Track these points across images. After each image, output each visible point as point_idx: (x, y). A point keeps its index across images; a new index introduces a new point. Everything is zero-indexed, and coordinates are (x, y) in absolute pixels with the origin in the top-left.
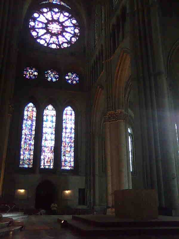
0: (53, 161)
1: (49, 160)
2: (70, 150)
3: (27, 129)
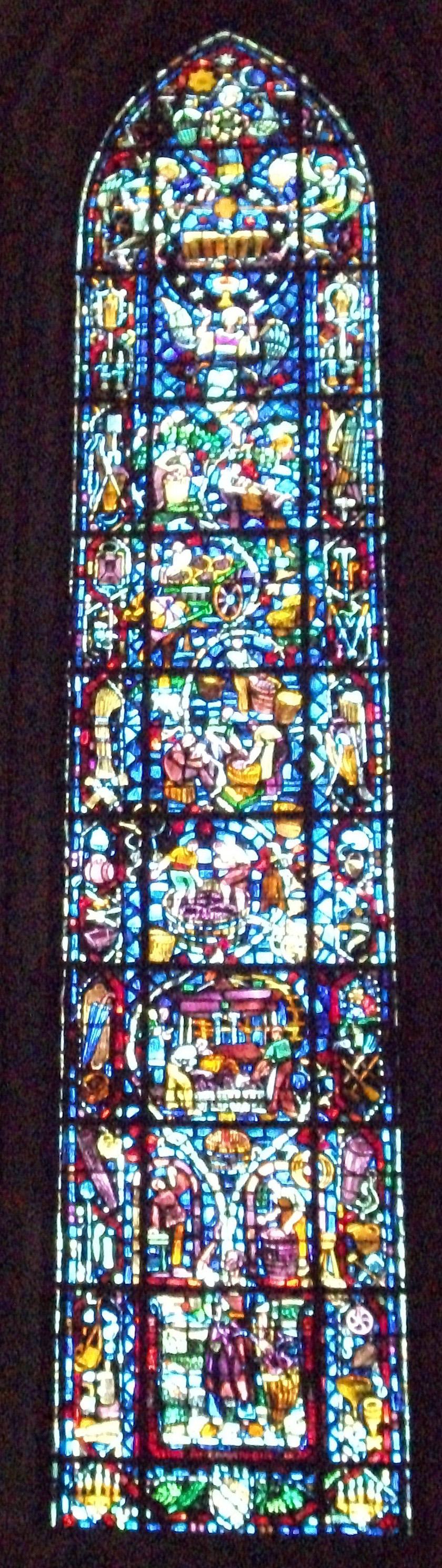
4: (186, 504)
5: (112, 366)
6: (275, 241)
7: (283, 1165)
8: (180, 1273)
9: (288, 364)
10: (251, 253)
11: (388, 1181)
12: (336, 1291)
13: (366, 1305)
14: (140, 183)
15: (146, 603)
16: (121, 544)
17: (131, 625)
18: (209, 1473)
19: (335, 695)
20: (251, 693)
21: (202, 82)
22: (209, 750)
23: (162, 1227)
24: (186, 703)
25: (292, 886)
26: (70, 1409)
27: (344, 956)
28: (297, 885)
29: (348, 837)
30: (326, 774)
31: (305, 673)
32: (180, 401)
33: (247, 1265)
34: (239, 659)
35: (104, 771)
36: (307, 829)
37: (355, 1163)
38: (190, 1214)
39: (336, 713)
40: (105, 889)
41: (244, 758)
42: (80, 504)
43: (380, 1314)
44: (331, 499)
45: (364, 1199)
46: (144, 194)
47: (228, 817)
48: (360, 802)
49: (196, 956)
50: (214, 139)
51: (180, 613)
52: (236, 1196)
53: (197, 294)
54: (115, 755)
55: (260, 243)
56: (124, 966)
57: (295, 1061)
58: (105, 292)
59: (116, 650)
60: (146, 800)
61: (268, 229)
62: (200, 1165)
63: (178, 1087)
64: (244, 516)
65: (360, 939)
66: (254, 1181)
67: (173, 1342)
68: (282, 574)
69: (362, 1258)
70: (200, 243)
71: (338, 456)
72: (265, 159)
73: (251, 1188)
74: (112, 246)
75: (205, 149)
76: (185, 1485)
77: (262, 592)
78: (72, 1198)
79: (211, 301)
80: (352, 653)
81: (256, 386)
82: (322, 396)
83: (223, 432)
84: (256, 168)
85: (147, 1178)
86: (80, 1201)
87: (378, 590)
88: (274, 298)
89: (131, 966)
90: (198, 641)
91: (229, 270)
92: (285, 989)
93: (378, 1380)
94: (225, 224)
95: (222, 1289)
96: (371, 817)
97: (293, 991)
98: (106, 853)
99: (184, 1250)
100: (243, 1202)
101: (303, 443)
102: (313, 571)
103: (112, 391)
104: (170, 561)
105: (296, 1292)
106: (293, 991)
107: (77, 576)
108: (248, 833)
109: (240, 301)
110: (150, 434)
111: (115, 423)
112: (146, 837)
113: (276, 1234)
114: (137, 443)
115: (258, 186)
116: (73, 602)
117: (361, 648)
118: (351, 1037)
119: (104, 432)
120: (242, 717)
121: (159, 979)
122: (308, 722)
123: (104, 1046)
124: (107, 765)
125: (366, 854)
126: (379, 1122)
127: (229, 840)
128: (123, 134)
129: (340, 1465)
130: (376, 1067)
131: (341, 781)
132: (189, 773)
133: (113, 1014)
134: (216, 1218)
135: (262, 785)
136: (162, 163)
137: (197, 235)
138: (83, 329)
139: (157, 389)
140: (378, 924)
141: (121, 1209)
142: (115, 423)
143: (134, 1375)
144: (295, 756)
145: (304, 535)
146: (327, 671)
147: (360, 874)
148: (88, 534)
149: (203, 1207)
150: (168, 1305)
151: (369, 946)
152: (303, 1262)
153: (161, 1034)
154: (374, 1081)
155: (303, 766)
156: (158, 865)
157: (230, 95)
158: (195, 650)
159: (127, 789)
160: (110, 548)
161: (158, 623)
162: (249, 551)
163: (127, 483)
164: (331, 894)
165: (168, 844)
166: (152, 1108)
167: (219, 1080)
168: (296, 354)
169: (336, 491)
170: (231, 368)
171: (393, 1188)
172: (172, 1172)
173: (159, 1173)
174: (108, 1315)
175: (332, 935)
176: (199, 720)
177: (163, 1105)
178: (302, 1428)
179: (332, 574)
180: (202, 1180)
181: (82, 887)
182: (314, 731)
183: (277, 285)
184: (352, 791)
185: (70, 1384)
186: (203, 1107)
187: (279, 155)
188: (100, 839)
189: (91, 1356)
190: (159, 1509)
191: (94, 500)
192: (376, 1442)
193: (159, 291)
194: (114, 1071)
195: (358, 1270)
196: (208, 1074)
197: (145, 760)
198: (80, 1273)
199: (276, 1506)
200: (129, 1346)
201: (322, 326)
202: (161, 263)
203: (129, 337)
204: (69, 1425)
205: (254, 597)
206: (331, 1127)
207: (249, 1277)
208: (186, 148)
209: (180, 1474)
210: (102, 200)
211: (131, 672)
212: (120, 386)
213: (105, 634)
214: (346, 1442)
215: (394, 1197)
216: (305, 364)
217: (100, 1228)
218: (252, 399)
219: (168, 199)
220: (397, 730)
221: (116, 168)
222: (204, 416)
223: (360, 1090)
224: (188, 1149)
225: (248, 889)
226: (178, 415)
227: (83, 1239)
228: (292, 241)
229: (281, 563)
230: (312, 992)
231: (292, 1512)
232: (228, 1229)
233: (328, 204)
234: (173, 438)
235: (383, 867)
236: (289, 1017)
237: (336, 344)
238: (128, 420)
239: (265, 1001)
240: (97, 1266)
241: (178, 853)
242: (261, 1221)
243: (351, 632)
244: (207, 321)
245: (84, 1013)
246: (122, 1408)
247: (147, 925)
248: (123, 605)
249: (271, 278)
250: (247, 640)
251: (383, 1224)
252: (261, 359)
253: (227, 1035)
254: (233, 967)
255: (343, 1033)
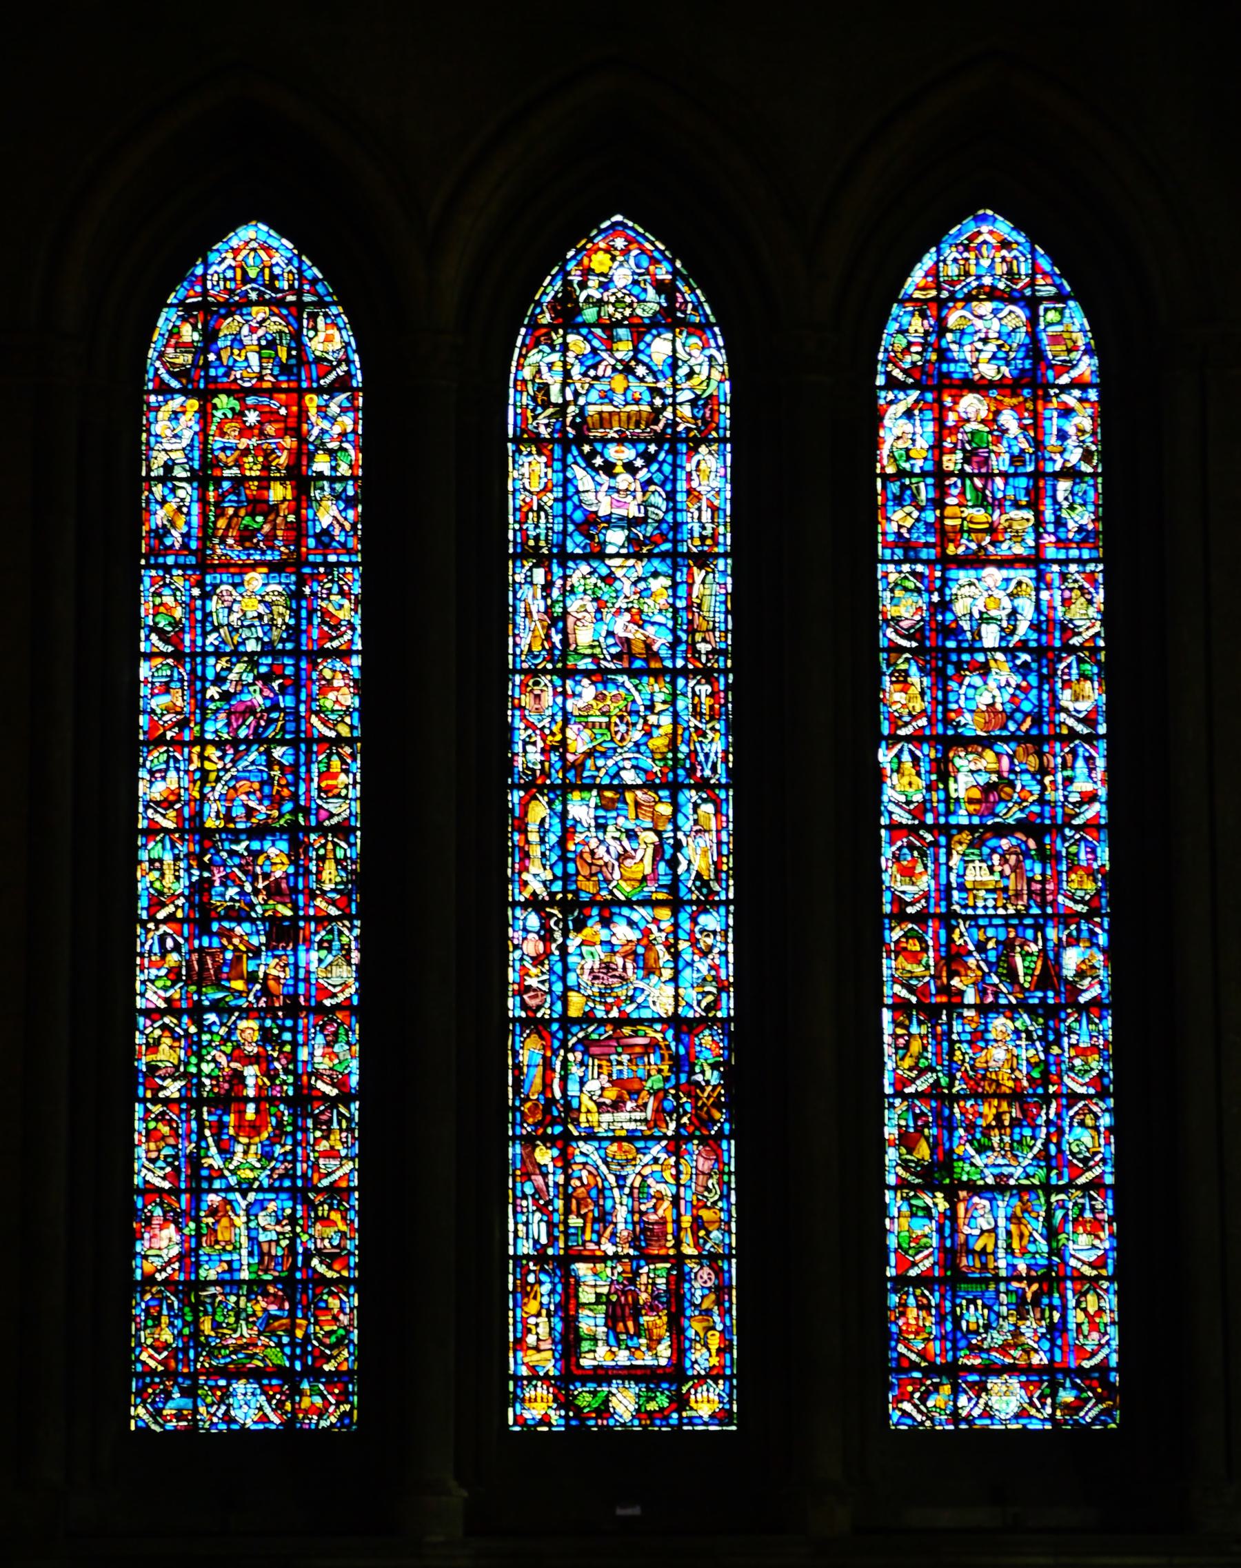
0: (720, 1290)
1: (656, 1275)
2: (1046, 1073)
3: (216, 727)
4: (592, 647)
5: (537, 526)
6: (657, 412)
7: (657, 1168)
8: (591, 1246)
9: (665, 526)
10: (637, 425)
11: (726, 1178)
12: (691, 1257)
13: (710, 1267)
14: (555, 357)
15: (563, 731)
16: (545, 680)
17: (554, 748)
18: (609, 1385)
19: (696, 806)
20: (637, 805)
21: (601, 263)
22: (608, 852)
23: (579, 1215)
24: (592, 813)
25: (665, 957)
26: (520, 1343)
27: (700, 1012)
28: (668, 957)
29: (703, 919)
30: (688, 870)
31: (675, 788)
32: (586, 558)
33: (634, 1241)
34: (629, 777)
35: (535, 867)
36: (675, 914)
37: (704, 1165)
38: (596, 1204)
39: (696, 822)
40: (537, 961)
41: (633, 858)
42: (516, 645)
43: (719, 1272)
44: (694, 643)
45: (710, 1191)
46: (558, 367)
47: (620, 904)
48: (712, 892)
49: (600, 1013)
50: (610, 316)
51: (587, 739)
52: (627, 1191)
53: (598, 461)
54: (543, 854)
55: (644, 415)
56: (552, 1020)
57: (666, 1091)
58: (530, 459)
59: (542, 770)
60: (565, 891)
61: (651, 404)
62: (603, 1168)
63: (589, 1111)
64: (632, 658)
65: (710, 998)
66: (639, 1179)
67: (586, 1296)
68: (659, 707)
69: (708, 1233)
70: (600, 413)
71: (699, 606)
72: (648, 338)
73: (637, 1184)
74: (535, 417)
75: (605, 328)
76: (594, 1393)
77: (646, 722)
78: (519, 1194)
79: (608, 468)
80: (707, 773)
81: (641, 544)
82: (689, 555)
83: (617, 585)
84: (642, 346)
85: (568, 1178)
86: (525, 1197)
87: (726, 721)
88: (655, 467)
89: (556, 1020)
90: (600, 763)
91: (621, 440)
92: (659, 1036)
93: (717, 1319)
94: (619, 399)
95: (617, 1257)
96: (721, 903)
97: (664, 1039)
98: (538, 933)
99: (593, 1231)
100: (630, 1195)
101: (675, 596)
102: (681, 704)
103: (537, 547)
104: (580, 695)
105: (666, 1259)
106: (664, 1039)
107: (513, 708)
108: (635, 917)
109: (630, 468)
110: (564, 586)
111: (539, 575)
112: (565, 920)
113: (653, 1218)
114: (556, 593)
115: (644, 364)
116: (512, 729)
117: (714, 769)
118: (703, 1072)
119: (531, 583)
120: (630, 825)
121: (575, 1029)
122: (676, 828)
123: (538, 1081)
124: (538, 862)
125: (714, 932)
126: (720, 1135)
127: (623, 922)
128: (542, 312)
129: (693, 1377)
130: (720, 1095)
131: (699, 876)
132: (594, 869)
133: (544, 1057)
134: (614, 1207)
135: (644, 879)
136: (571, 338)
137: (599, 408)
138: (515, 490)
139: (570, 547)
140: (722, 988)
141: (550, 1202)
142: (539, 575)
143: (562, 1319)
144: (667, 856)
145: (675, 673)
146: (689, 787)
147: (711, 948)
148: (522, 671)
149: (605, 1198)
150: (582, 1269)
151: (715, 1005)
152: (670, 1237)
153: (576, 1071)
154: (717, 1105)
155: (673, 863)
156: (573, 942)
157: (622, 277)
158: (598, 769)
159: (552, 882)
160: (537, 683)
161: (571, 749)
162: (636, 687)
163: (549, 627)
164: (690, 964)
165: (580, 926)
166: (571, 1127)
167: (617, 1106)
168: (669, 518)
169: (698, 637)
170: (623, 528)
171: (729, 1183)
172: (584, 1173)
173: (576, 1174)
174: (543, 1277)
175: (690, 994)
176: (602, 827)
177: (577, 1125)
178: (668, 1353)
179: (694, 706)
180: (605, 1179)
181: (522, 959)
182: (680, 835)
183: (657, 453)
184: (706, 884)
185: (519, 1326)
186: (605, 1126)
187: (659, 335)
188: (533, 921)
189: (533, 1307)
190: (579, 1410)
191: (524, 645)
192: (715, 1361)
193: (570, 459)
194: (546, 1099)
195: (706, 1242)
196: (608, 1102)
197: (564, 859)
198: (526, 1248)
199: (652, 1406)
200: (558, 1298)
201: (689, 492)
202: (571, 432)
203: (548, 499)
204: (520, 1354)
205: (639, 726)
206: (689, 1139)
207: (635, 1248)
208: (589, 326)
209: (591, 1386)
210: (527, 373)
211: (553, 787)
212: (542, 543)
213: (534, 756)
214: (696, 1362)
215: (729, 1189)
216: (676, 526)
217: (538, 1215)
218: (638, 556)
219: (576, 371)
220: (737, 834)
221: (537, 344)
222: (604, 571)
223: (708, 1112)
224: (595, 1157)
225: (635, 961)
226: (584, 568)
227: (526, 1224)
228: (668, 414)
229: (659, 697)
230: (677, 1038)
231: (662, 1409)
232: (622, 1213)
233: (695, 381)
234: (581, 589)
235: (726, 943)
236: (662, 1058)
237: (699, 509)
238: (549, 572)
239: (645, 1046)
240: (536, 1242)
241: (586, 931)
242: (643, 1208)
243: (707, 756)
244: (605, 488)
245: (524, 1057)
246: (554, 1342)
247: (567, 989)
248: (547, 731)
249: (652, 448)
250: (634, 762)
251: (721, 1209)
252: (642, 521)
253: (621, 1071)
254: (625, 1020)
255: (697, 1069)
